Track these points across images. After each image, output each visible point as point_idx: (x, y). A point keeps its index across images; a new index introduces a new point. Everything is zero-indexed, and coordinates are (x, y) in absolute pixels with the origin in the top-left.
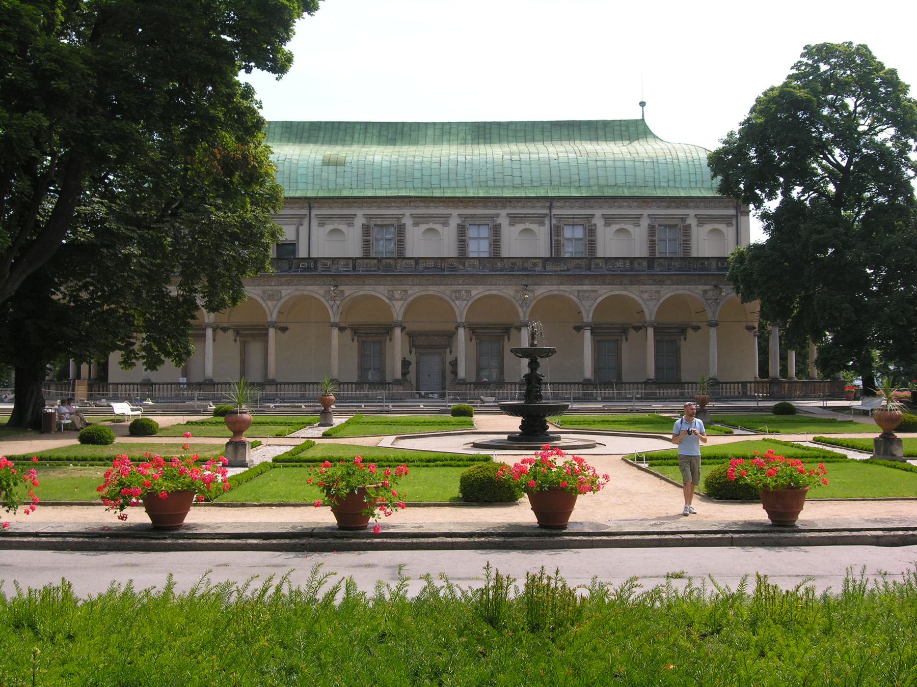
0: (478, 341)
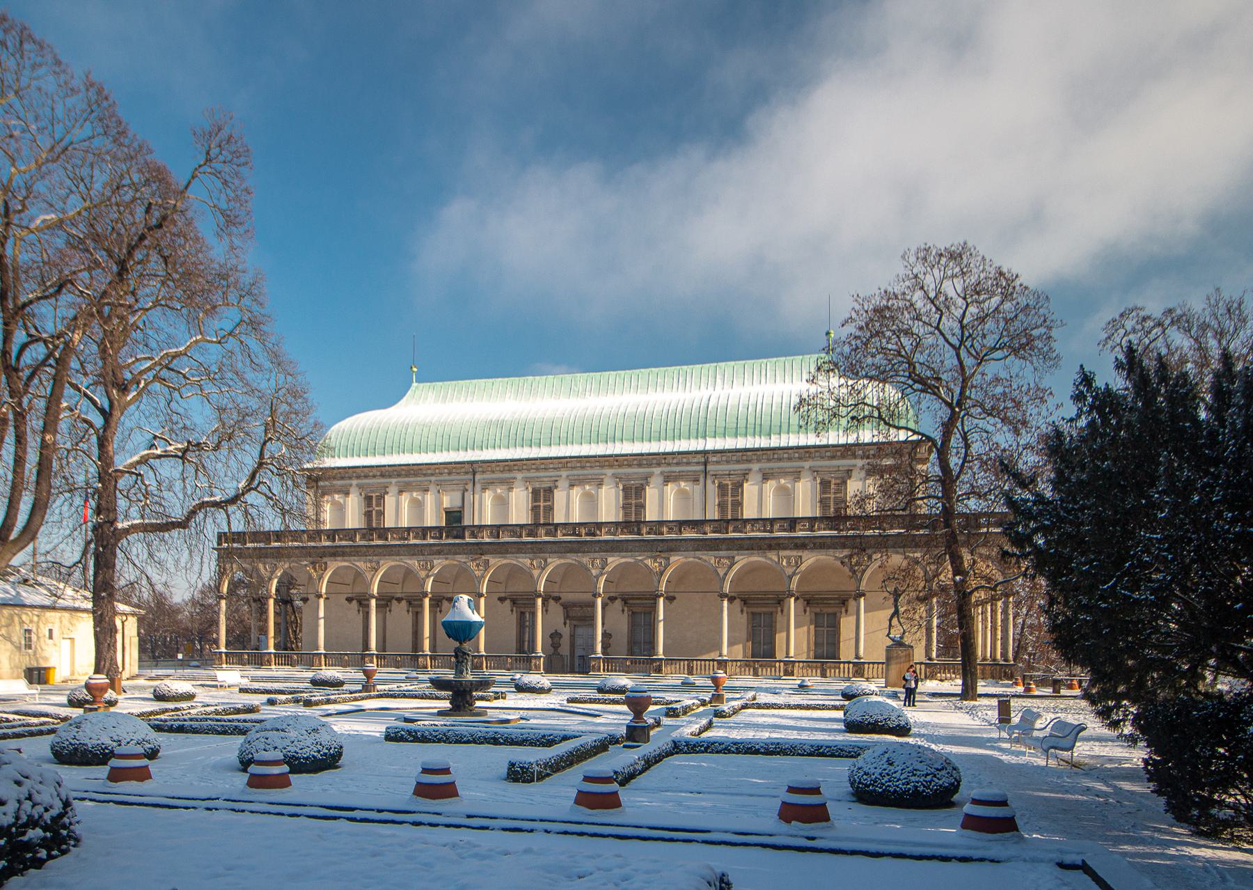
0: (630, 613)
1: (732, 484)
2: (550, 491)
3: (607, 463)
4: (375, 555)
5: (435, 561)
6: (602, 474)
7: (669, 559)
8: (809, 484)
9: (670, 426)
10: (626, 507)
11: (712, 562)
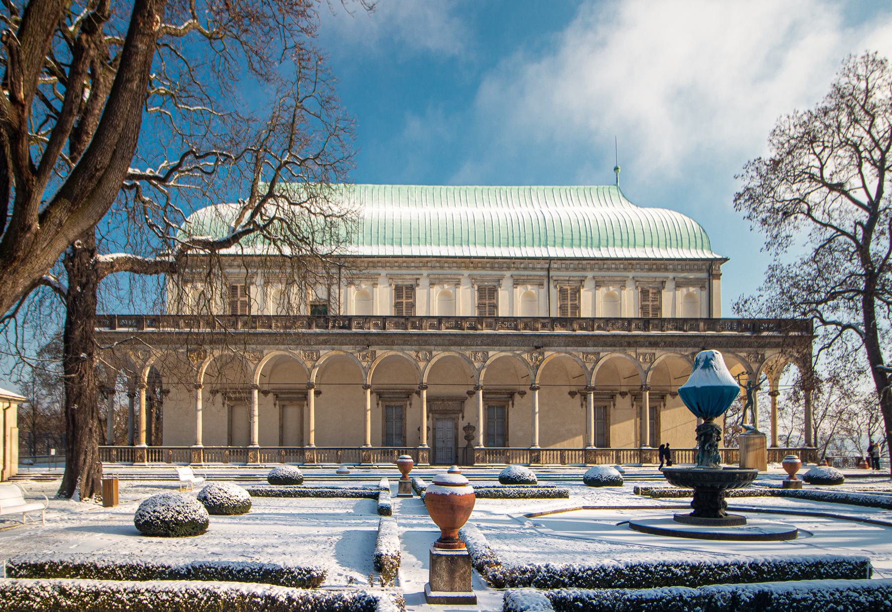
1: (571, 289)
2: (411, 289)
3: (463, 265)
4: (259, 344)
5: (321, 352)
6: (460, 275)
7: (543, 354)
8: (632, 292)
9: (516, 234)
10: (480, 306)
11: (581, 357)
